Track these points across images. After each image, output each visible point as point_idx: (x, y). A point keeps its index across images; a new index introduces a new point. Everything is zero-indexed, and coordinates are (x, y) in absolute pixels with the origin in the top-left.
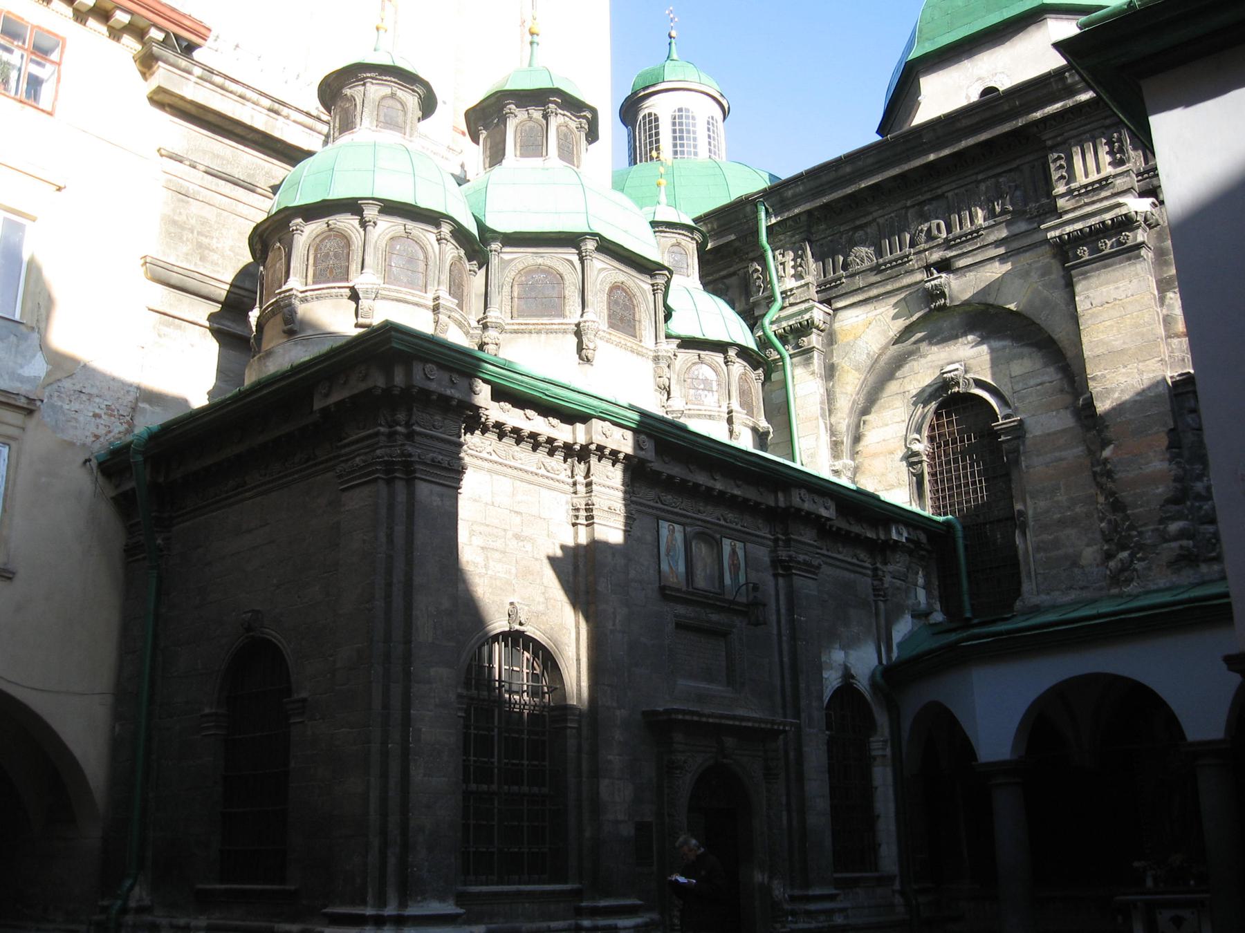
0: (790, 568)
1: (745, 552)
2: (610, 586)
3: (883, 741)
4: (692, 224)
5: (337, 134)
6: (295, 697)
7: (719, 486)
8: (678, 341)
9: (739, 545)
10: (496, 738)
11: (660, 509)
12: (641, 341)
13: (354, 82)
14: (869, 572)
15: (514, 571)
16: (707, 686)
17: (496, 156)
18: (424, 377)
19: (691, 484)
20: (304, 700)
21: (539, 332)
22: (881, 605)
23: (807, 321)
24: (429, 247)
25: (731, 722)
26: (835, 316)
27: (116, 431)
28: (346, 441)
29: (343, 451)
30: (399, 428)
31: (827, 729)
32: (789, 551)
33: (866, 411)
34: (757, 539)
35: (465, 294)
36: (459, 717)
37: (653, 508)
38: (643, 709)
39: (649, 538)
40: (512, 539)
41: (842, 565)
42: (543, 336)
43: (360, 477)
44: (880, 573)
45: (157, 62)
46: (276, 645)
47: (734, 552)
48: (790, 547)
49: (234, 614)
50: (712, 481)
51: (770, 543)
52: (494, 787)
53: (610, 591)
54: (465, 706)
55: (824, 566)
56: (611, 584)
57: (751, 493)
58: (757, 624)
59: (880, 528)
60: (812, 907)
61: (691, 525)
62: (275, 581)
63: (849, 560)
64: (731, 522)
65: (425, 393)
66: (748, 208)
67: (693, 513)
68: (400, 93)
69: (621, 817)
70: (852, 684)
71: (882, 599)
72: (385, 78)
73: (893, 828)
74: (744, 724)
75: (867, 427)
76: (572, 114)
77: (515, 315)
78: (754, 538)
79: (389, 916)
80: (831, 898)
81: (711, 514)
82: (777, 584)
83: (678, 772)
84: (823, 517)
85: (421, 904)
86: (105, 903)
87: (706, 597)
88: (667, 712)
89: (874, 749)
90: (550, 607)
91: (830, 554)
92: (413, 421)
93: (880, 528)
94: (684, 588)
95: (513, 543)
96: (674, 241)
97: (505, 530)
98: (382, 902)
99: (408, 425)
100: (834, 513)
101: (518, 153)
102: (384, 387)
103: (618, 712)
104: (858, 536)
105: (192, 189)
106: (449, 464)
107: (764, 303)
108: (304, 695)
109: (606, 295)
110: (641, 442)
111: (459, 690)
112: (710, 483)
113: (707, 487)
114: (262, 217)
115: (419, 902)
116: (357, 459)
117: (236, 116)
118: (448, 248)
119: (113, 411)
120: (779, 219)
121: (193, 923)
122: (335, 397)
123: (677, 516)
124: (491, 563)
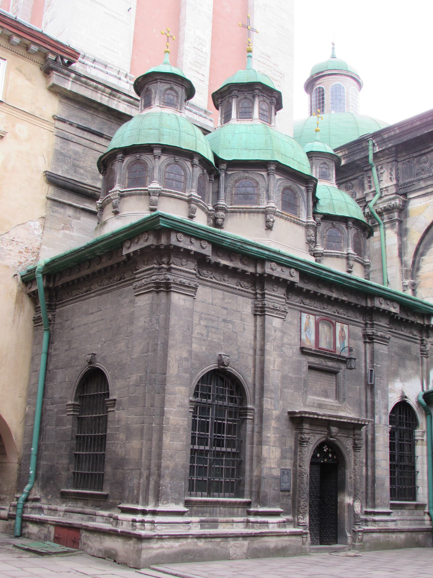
0: (373, 339)
1: (349, 330)
3: (422, 432)
4: (332, 152)
5: (143, 108)
6: (111, 398)
7: (335, 295)
8: (322, 216)
9: (345, 326)
10: (210, 422)
11: (302, 307)
12: (299, 217)
13: (152, 81)
14: (419, 341)
15: (222, 338)
16: (325, 400)
17: (227, 118)
18: (176, 240)
19: (319, 294)
20: (115, 400)
21: (245, 212)
22: (425, 359)
23: (393, 204)
24: (187, 169)
25: (335, 419)
26: (409, 202)
27: (30, 260)
28: (138, 271)
29: (137, 276)
30: (164, 266)
31: (390, 424)
32: (373, 330)
33: (422, 255)
35: (206, 192)
36: (190, 412)
37: (298, 306)
38: (289, 410)
39: (296, 322)
40: (220, 322)
41: (404, 337)
42: (247, 215)
43: (144, 289)
44: (425, 342)
45: (52, 71)
46: (102, 371)
47: (342, 329)
48: (373, 328)
49: (84, 355)
50: (331, 293)
51: (363, 325)
52: (207, 448)
54: (194, 406)
55: (392, 339)
57: (353, 300)
58: (351, 369)
59: (425, 318)
60: (377, 518)
61: (317, 315)
62: (103, 339)
63: (408, 335)
64: (341, 314)
65: (177, 249)
66: (364, 145)
68: (175, 87)
69: (273, 466)
70: (405, 401)
71: (425, 356)
72: (167, 79)
73: (426, 478)
74: (342, 420)
75: (423, 263)
76: (267, 95)
77: (233, 203)
79: (149, 511)
80: (388, 514)
81: (330, 310)
82: (365, 347)
83: (305, 444)
84: (392, 312)
85: (166, 505)
86: (18, 496)
87: (326, 353)
88: (300, 413)
89: (416, 436)
90: (240, 357)
91: (397, 331)
92: (170, 262)
93: (425, 318)
94: (313, 349)
95: (223, 323)
96: (322, 162)
97: (218, 317)
98: (146, 503)
99: (168, 264)
100: (399, 310)
101: (238, 116)
102: (156, 244)
103: (274, 412)
104: (412, 322)
105: (70, 136)
106: (189, 284)
107: (371, 194)
108: (115, 397)
109: (281, 193)
110: (291, 273)
111: (191, 398)
112: (330, 294)
113: (328, 296)
114: (106, 150)
115: (165, 504)
116: (143, 280)
117: (93, 99)
118: (197, 169)
119: (29, 250)
120: (380, 149)
121: (59, 508)
122: (133, 249)
124: (210, 334)
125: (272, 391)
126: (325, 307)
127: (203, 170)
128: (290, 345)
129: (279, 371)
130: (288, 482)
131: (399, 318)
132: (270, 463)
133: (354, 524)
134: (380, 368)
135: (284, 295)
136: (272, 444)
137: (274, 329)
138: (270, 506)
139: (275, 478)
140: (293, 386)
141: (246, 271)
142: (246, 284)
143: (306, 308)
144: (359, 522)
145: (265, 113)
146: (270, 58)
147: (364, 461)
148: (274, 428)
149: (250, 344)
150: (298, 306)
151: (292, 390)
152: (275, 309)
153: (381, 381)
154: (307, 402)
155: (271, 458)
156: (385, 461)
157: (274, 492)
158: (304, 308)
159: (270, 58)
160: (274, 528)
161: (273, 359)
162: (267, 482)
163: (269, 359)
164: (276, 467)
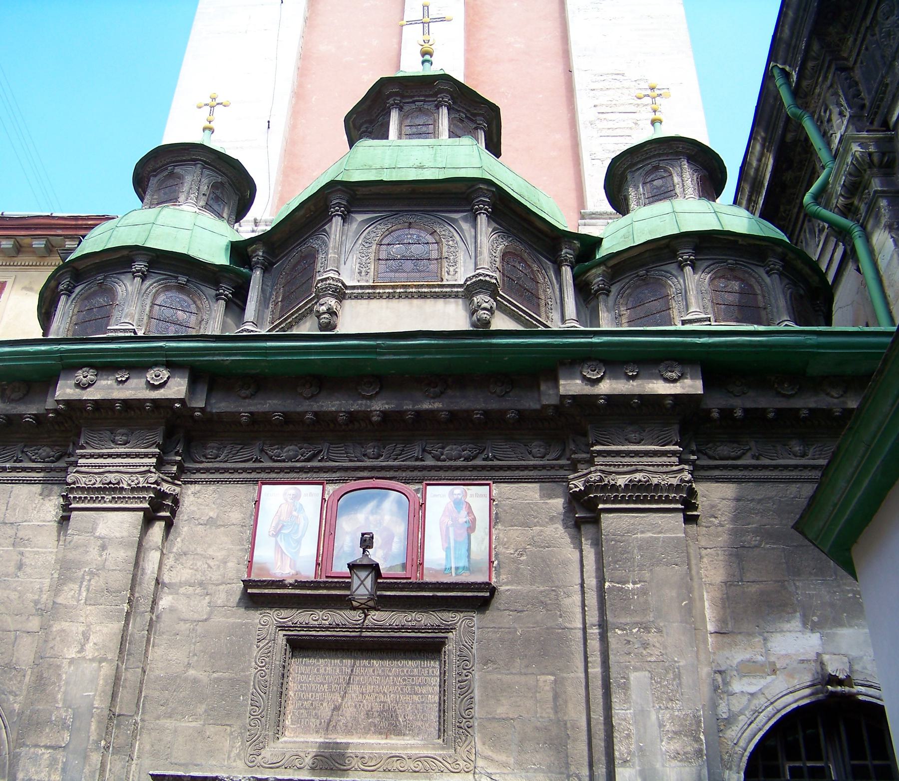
1: (491, 500)
2: (84, 594)
7: (379, 405)
16: (362, 741)
34: (526, 473)
37: (245, 470)
56: (88, 590)
67: (351, 461)
78: (517, 473)
112: (356, 406)
113: (350, 413)
123: (307, 472)
125: (64, 726)
126: (370, 451)
127: (176, 278)
131: (739, 413)
134: (644, 592)
135: (158, 446)
137: (100, 542)
140: (201, 709)
141: (21, 416)
142: (45, 451)
143: (282, 470)
145: (424, 129)
146: (623, 75)
149: (36, 602)
150: (245, 470)
151: (196, 720)
152: (113, 489)
154: (268, 753)
158: (272, 470)
159: (623, 75)
161: (81, 629)
163: (64, 631)
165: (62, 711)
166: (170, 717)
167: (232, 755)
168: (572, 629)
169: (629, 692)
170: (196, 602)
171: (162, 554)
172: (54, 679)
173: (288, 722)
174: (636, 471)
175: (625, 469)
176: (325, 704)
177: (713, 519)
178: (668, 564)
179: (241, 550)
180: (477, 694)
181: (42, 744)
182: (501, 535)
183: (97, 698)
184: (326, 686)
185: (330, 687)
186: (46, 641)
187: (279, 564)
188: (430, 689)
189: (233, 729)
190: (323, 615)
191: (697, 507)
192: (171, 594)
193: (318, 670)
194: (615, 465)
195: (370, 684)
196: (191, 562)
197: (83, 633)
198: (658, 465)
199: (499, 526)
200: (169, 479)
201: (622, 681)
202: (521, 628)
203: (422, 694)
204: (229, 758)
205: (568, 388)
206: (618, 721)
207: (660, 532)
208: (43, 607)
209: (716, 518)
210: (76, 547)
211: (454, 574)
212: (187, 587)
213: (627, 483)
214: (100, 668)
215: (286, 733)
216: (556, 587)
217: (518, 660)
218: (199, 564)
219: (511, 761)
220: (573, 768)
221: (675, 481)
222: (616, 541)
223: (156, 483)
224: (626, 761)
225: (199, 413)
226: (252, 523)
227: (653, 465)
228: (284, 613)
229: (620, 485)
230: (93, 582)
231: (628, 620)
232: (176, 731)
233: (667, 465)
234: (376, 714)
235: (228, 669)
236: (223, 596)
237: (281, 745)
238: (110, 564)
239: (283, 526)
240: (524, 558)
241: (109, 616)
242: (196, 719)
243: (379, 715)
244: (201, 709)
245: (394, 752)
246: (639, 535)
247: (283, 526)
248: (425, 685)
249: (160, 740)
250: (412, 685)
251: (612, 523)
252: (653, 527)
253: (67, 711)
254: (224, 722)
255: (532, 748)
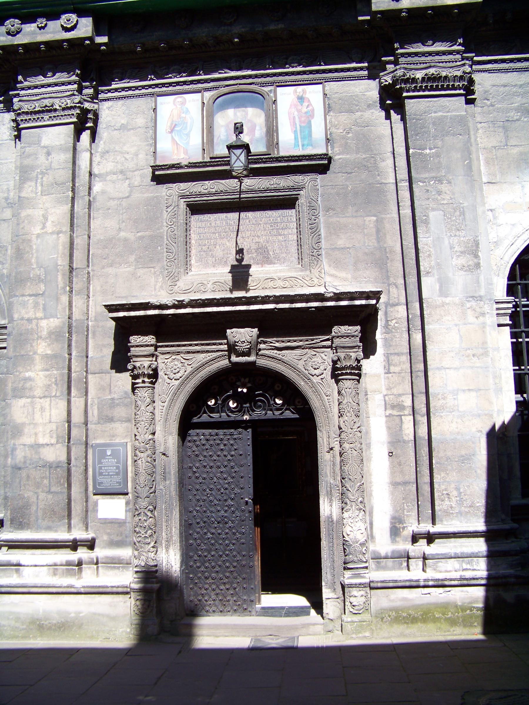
2: (40, 188)
53: (39, 193)
56: (42, 185)
69: (41, 441)
103: (44, 323)
125: (39, 280)
128: (122, 172)
129: (58, 233)
130: (118, 474)
132: (36, 434)
133: (345, 569)
134: (438, 155)
136: (38, 392)
137: (45, 150)
138: (38, 529)
139: (51, 466)
140: (132, 258)
144: (353, 562)
147: (408, 402)
148: (46, 357)
153: (444, 187)
154: (181, 284)
155: (35, 425)
156: (474, 394)
157: (50, 496)
160: (37, 576)
161: (41, 212)
162: (28, 477)
163: (29, 215)
164: (54, 441)
165: (37, 270)
166: (111, 266)
167: (157, 287)
168: (387, 184)
169: (429, 226)
170: (119, 185)
171: (91, 154)
172: (27, 249)
173: (193, 262)
174: (430, 67)
175: (422, 66)
176: (218, 247)
177: (486, 101)
178: (454, 135)
179: (148, 145)
180: (323, 232)
181: (27, 294)
182: (333, 120)
183: (59, 259)
184: (217, 235)
185: (220, 235)
186: (18, 224)
187: (176, 152)
188: (290, 231)
189: (156, 270)
190: (210, 185)
191: (475, 93)
192: (101, 181)
193: (210, 224)
194: (414, 64)
195: (248, 230)
196: (113, 158)
197: (43, 216)
198: (446, 62)
199: (331, 113)
200: (89, 99)
201: (424, 218)
202: (351, 185)
203: (284, 235)
204: (155, 289)
205: (378, 5)
206: (422, 246)
207: (448, 112)
208: (12, 201)
209: (488, 100)
210: (29, 156)
211: (301, 149)
212: (112, 175)
213: (423, 76)
214: (58, 238)
215: (193, 269)
216: (374, 154)
217: (350, 207)
218: (118, 158)
219: (349, 276)
220: (391, 279)
221: (459, 74)
222: (417, 120)
223: (80, 102)
224: (428, 273)
225: (104, 47)
226: (153, 125)
227: (442, 62)
228: (183, 185)
229: (418, 78)
230: (44, 179)
231: (427, 175)
232: (116, 275)
233: (453, 62)
234: (253, 251)
235: (148, 229)
236: (138, 179)
237: (190, 278)
238: (55, 165)
239: (176, 125)
240: (350, 135)
241: (59, 202)
242: (130, 265)
243: (256, 251)
244: (132, 258)
245: (269, 276)
246: (433, 115)
247: (176, 125)
248: (286, 229)
249: (106, 282)
250: (277, 229)
251: (413, 106)
252: (443, 108)
253: (40, 270)
254: (149, 266)
255: (363, 267)
